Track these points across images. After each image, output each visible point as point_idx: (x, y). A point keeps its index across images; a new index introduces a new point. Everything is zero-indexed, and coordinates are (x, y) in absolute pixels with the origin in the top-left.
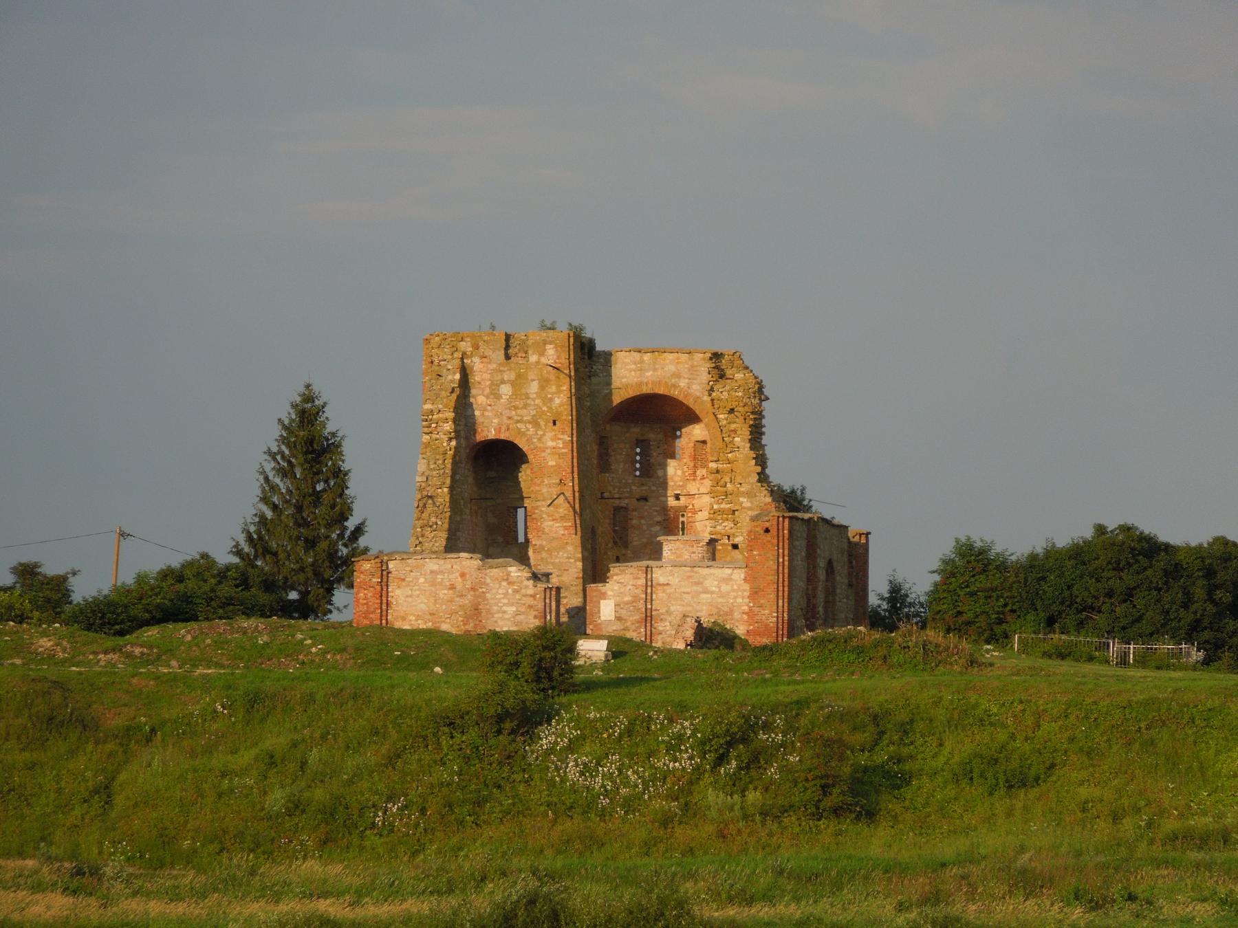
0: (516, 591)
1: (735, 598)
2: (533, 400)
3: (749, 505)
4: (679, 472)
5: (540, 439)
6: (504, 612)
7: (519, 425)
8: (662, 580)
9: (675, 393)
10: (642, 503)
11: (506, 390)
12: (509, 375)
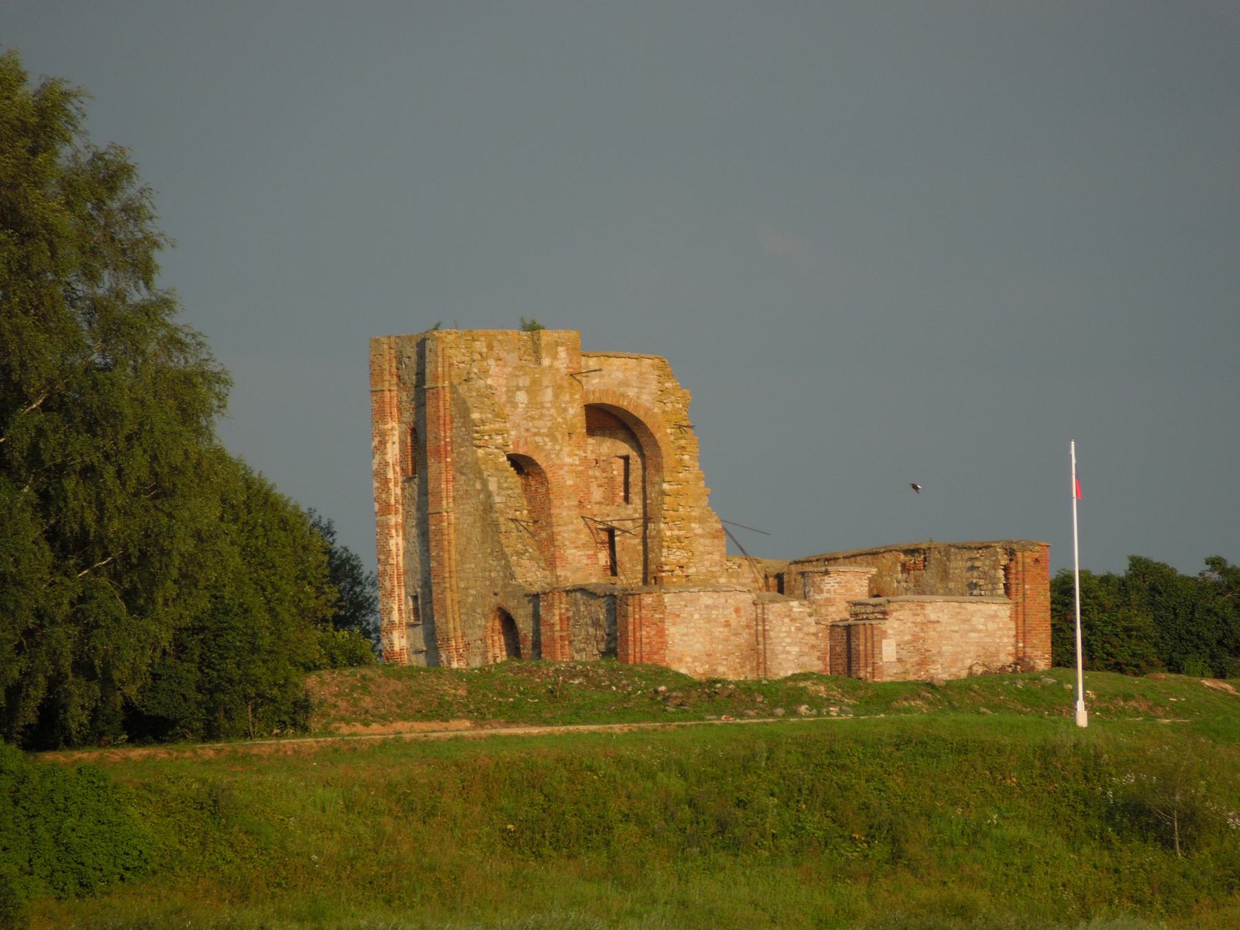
0: (799, 629)
1: (1000, 637)
2: (548, 409)
6: (788, 652)
7: (537, 439)
8: (933, 617)
9: (624, 404)
12: (524, 381)
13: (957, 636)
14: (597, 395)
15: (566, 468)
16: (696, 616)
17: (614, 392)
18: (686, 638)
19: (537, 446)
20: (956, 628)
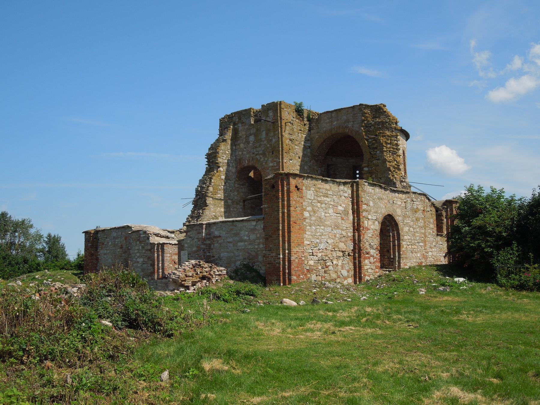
0: (143, 247)
1: (259, 244)
5: (266, 163)
6: (138, 262)
7: (258, 157)
8: (217, 233)
11: (252, 138)
13: (231, 245)
15: (270, 169)
16: (110, 243)
18: (105, 256)
20: (231, 240)
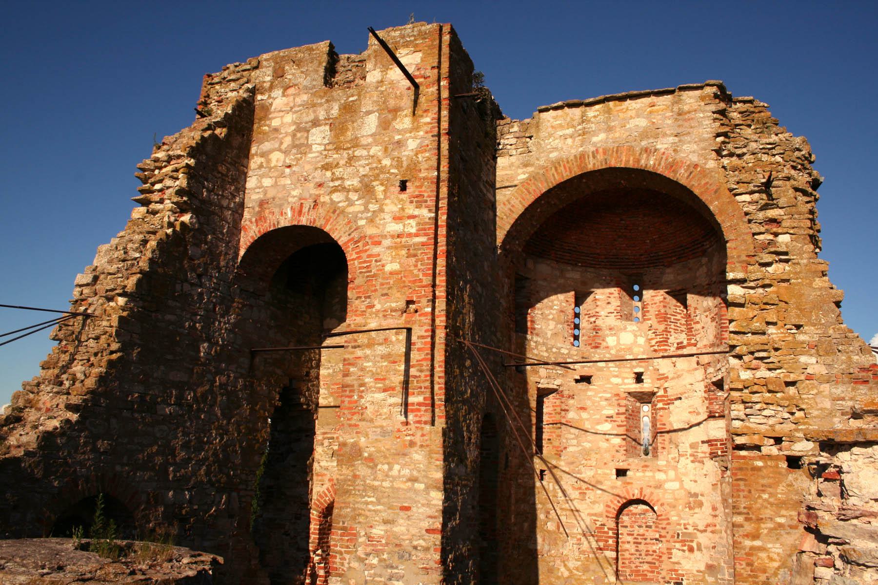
2: (367, 147)
3: (823, 370)
4: (641, 341)
5: (371, 221)
7: (336, 197)
9: (649, 163)
10: (583, 386)
14: (600, 157)
15: (387, 242)
17: (631, 149)
19: (335, 210)
